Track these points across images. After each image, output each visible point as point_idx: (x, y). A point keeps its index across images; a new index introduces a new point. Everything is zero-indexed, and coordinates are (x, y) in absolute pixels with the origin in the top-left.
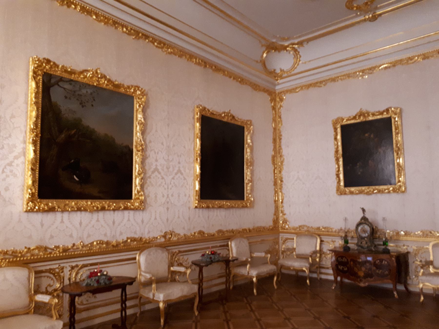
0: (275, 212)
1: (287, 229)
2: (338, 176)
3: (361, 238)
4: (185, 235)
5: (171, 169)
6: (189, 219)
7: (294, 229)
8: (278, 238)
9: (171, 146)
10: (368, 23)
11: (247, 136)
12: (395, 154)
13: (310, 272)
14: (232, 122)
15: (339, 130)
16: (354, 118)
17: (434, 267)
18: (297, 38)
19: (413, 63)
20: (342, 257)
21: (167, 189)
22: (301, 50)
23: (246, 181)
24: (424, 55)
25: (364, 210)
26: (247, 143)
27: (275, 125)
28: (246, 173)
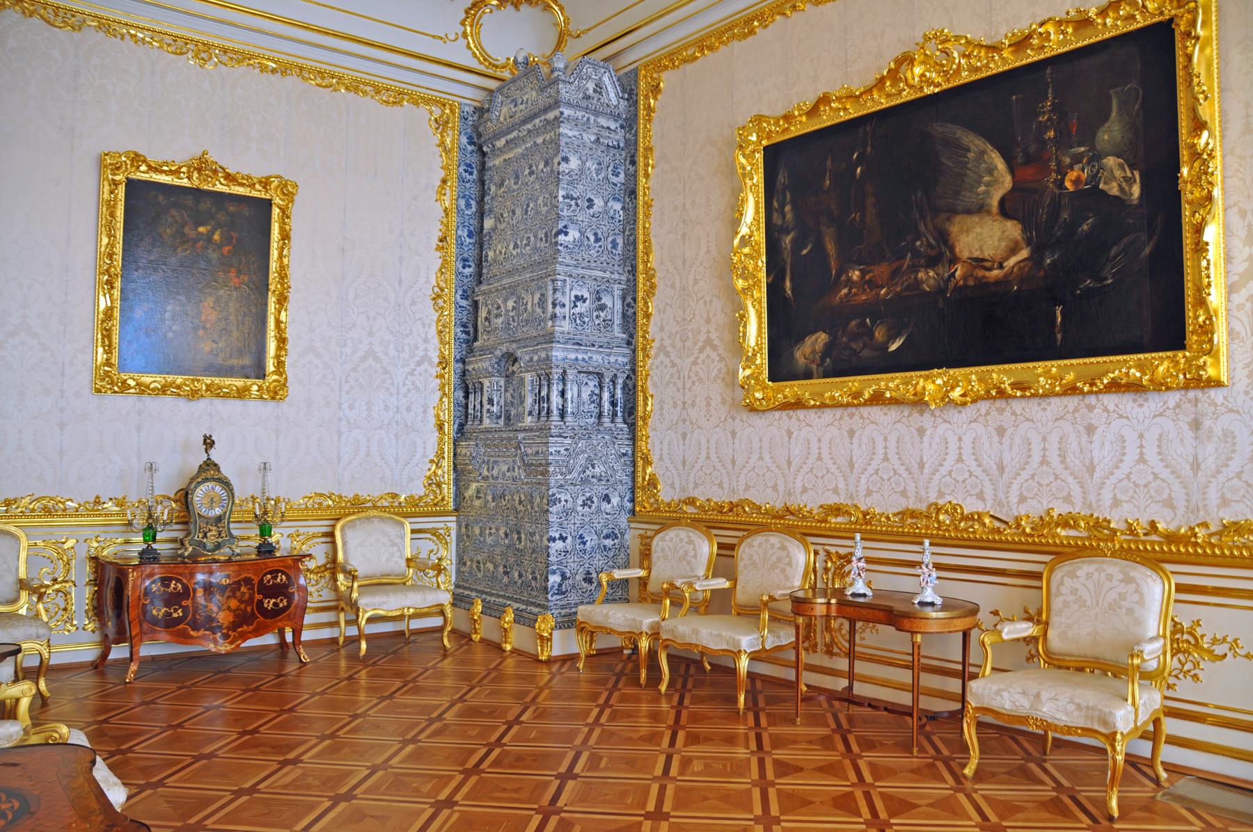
25: (209, 443)
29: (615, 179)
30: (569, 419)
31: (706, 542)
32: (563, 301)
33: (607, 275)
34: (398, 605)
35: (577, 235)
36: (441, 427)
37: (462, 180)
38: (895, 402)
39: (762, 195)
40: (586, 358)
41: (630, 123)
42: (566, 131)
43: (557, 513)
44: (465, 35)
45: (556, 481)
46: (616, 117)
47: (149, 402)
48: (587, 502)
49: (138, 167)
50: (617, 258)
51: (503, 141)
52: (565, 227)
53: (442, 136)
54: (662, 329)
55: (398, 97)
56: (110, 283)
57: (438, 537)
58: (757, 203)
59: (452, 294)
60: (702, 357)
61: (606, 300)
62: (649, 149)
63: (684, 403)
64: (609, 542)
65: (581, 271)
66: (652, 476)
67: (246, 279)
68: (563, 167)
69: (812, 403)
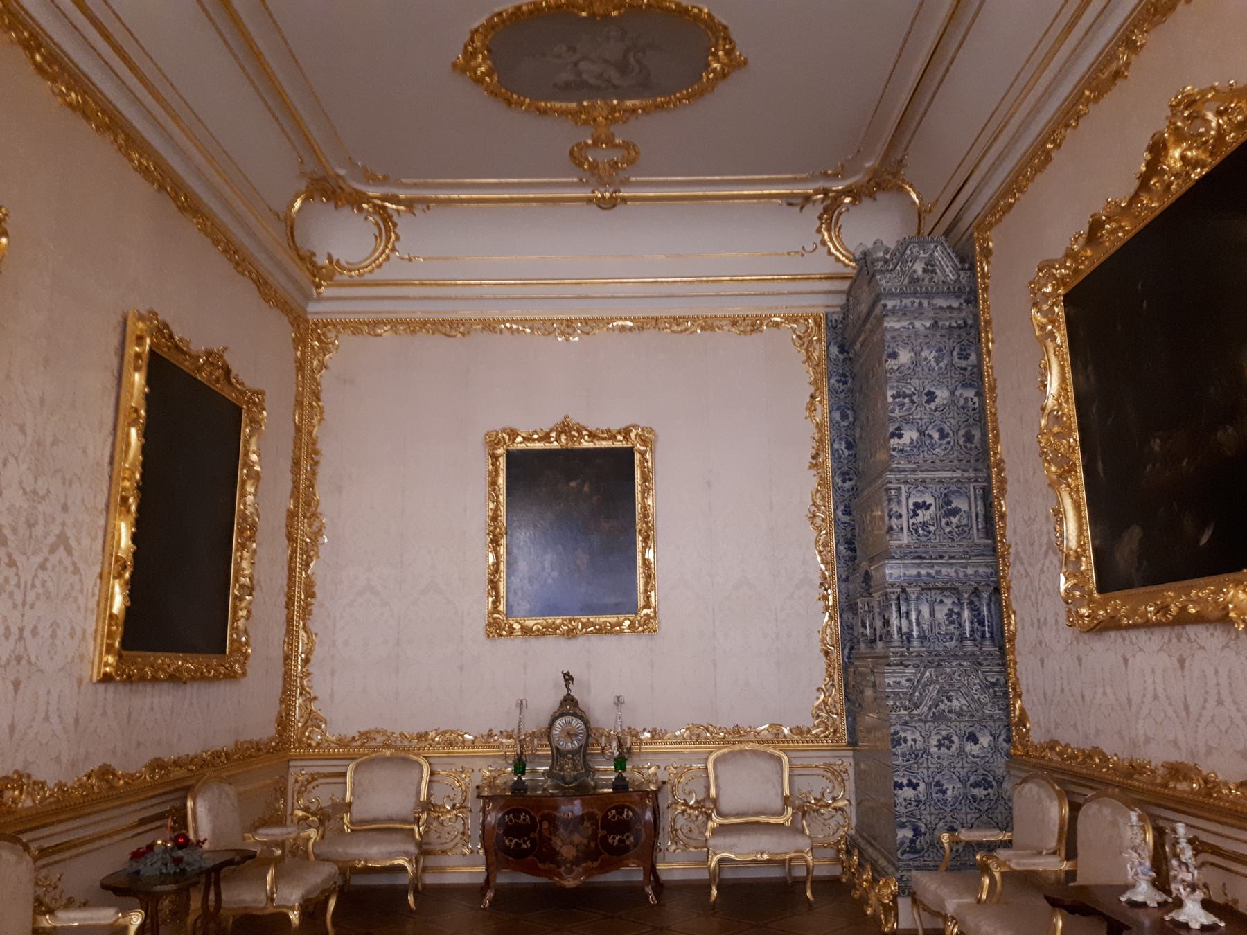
0: (284, 691)
3: (558, 754)
4: (60, 786)
5: (39, 531)
6: (77, 721)
7: (341, 743)
9: (49, 440)
10: (594, 207)
12: (639, 539)
15: (502, 462)
17: (720, 814)
18: (406, 186)
20: (516, 812)
21: (20, 607)
22: (405, 223)
23: (234, 591)
24: (705, 319)
25: (568, 678)
26: (246, 464)
27: (301, 418)
28: (238, 564)
29: (964, 363)
30: (916, 644)
31: (1056, 803)
33: (958, 474)
35: (915, 435)
36: (827, 653)
37: (833, 391)
38: (1199, 619)
39: (1067, 357)
40: (932, 572)
42: (891, 324)
43: (903, 755)
44: (824, 243)
45: (899, 717)
47: (535, 644)
48: (945, 742)
50: (974, 453)
51: (858, 345)
52: (899, 429)
53: (807, 351)
54: (1015, 532)
55: (753, 325)
56: (495, 542)
57: (833, 774)
58: (1062, 367)
61: (959, 503)
62: (988, 323)
64: (979, 792)
65: (920, 475)
66: (1022, 709)
68: (891, 364)
69: (1125, 621)
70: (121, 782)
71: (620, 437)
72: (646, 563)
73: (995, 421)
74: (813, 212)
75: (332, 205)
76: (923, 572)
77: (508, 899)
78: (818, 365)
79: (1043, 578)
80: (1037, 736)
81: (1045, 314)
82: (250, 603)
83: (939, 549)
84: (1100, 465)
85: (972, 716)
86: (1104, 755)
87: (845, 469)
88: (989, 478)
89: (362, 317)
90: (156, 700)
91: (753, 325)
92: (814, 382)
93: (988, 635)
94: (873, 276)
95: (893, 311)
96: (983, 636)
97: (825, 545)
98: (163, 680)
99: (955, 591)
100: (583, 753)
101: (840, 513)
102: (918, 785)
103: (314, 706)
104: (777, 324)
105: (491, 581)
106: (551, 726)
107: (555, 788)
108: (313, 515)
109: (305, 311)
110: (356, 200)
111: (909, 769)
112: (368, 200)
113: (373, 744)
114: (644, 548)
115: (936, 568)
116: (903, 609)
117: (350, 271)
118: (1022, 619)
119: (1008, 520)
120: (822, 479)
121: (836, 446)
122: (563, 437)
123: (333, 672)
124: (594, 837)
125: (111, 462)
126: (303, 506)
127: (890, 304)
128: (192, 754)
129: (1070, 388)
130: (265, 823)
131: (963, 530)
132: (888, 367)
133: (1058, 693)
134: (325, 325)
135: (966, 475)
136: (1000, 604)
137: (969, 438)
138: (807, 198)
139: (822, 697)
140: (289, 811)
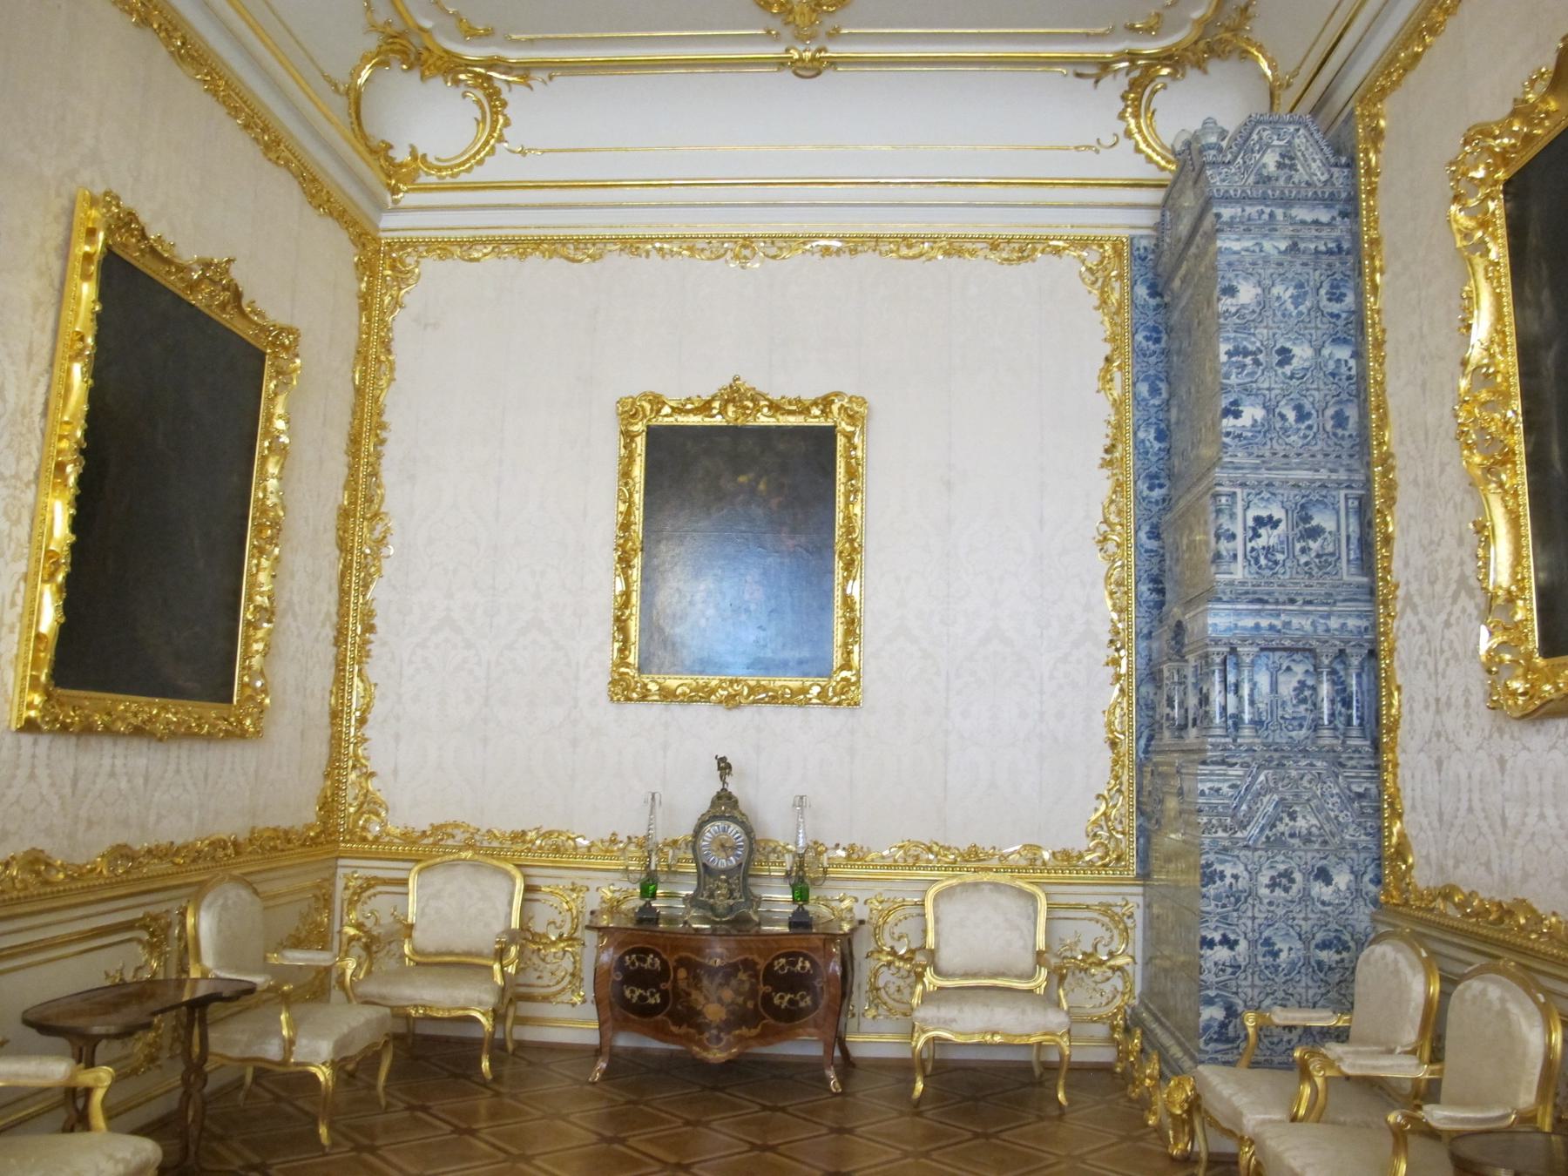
1: (377, 839)
2: (621, 624)
3: (706, 871)
7: (407, 838)
8: (331, 880)
11: (271, 400)
12: (839, 565)
13: (498, 1016)
14: (225, 318)
15: (640, 444)
16: (705, 408)
19: (914, 257)
20: (642, 952)
22: (517, 99)
23: (246, 614)
25: (724, 767)
26: (267, 433)
27: (363, 377)
28: (253, 576)
29: (1335, 307)
30: (1246, 732)
32: (1233, 529)
33: (1323, 475)
34: (979, 1025)
35: (1259, 414)
36: (1113, 744)
37: (1139, 353)
39: (1506, 281)
40: (1277, 623)
41: (1350, 209)
42: (1227, 244)
43: (1218, 898)
44: (1128, 134)
45: (1215, 841)
46: (1329, 201)
48: (1282, 880)
49: (659, 411)
50: (1347, 443)
52: (1235, 403)
53: (1102, 292)
54: (1406, 564)
55: (1024, 249)
57: (1112, 918)
58: (1498, 297)
59: (1126, 534)
60: (1457, 610)
62: (1375, 242)
63: (1438, 700)
65: (1265, 475)
66: (1402, 835)
67: (803, 539)
68: (1226, 303)
70: (61, 876)
71: (816, 411)
72: (848, 602)
73: (1381, 394)
74: (1115, 85)
75: (416, 74)
76: (1264, 623)
77: (623, 1069)
78: (1117, 313)
79: (1449, 634)
80: (1423, 878)
81: (1471, 213)
82: (270, 632)
83: (1291, 588)
84: (1556, 451)
85: (1325, 843)
86: (1534, 911)
87: (1154, 469)
88: (1368, 482)
89: (453, 234)
90: (119, 762)
91: (1024, 249)
92: (1112, 339)
93: (1355, 722)
94: (1202, 171)
95: (1231, 224)
96: (1349, 723)
97: (1119, 584)
98: (124, 734)
99: (1311, 652)
100: (744, 875)
101: (1143, 535)
102: (1236, 942)
103: (372, 785)
104: (1057, 251)
105: (618, 619)
106: (698, 832)
107: (704, 920)
108: (376, 515)
109: (377, 229)
110: (451, 67)
111: (1224, 918)
112: (467, 65)
113: (450, 842)
114: (846, 579)
115: (1283, 617)
116: (1231, 679)
117: (440, 169)
118: (1411, 698)
119: (1397, 546)
120: (1119, 484)
121: (1141, 435)
122: (731, 409)
123: (397, 738)
124: (753, 993)
125: (45, 414)
126: (360, 505)
127: (1227, 212)
128: (179, 842)
129: (1510, 330)
130: (297, 943)
131: (1326, 561)
132: (1221, 307)
133: (1462, 813)
134: (404, 246)
135: (1334, 476)
136: (1377, 677)
137: (1340, 419)
138: (1105, 66)
139: (1103, 808)
140: (337, 928)
